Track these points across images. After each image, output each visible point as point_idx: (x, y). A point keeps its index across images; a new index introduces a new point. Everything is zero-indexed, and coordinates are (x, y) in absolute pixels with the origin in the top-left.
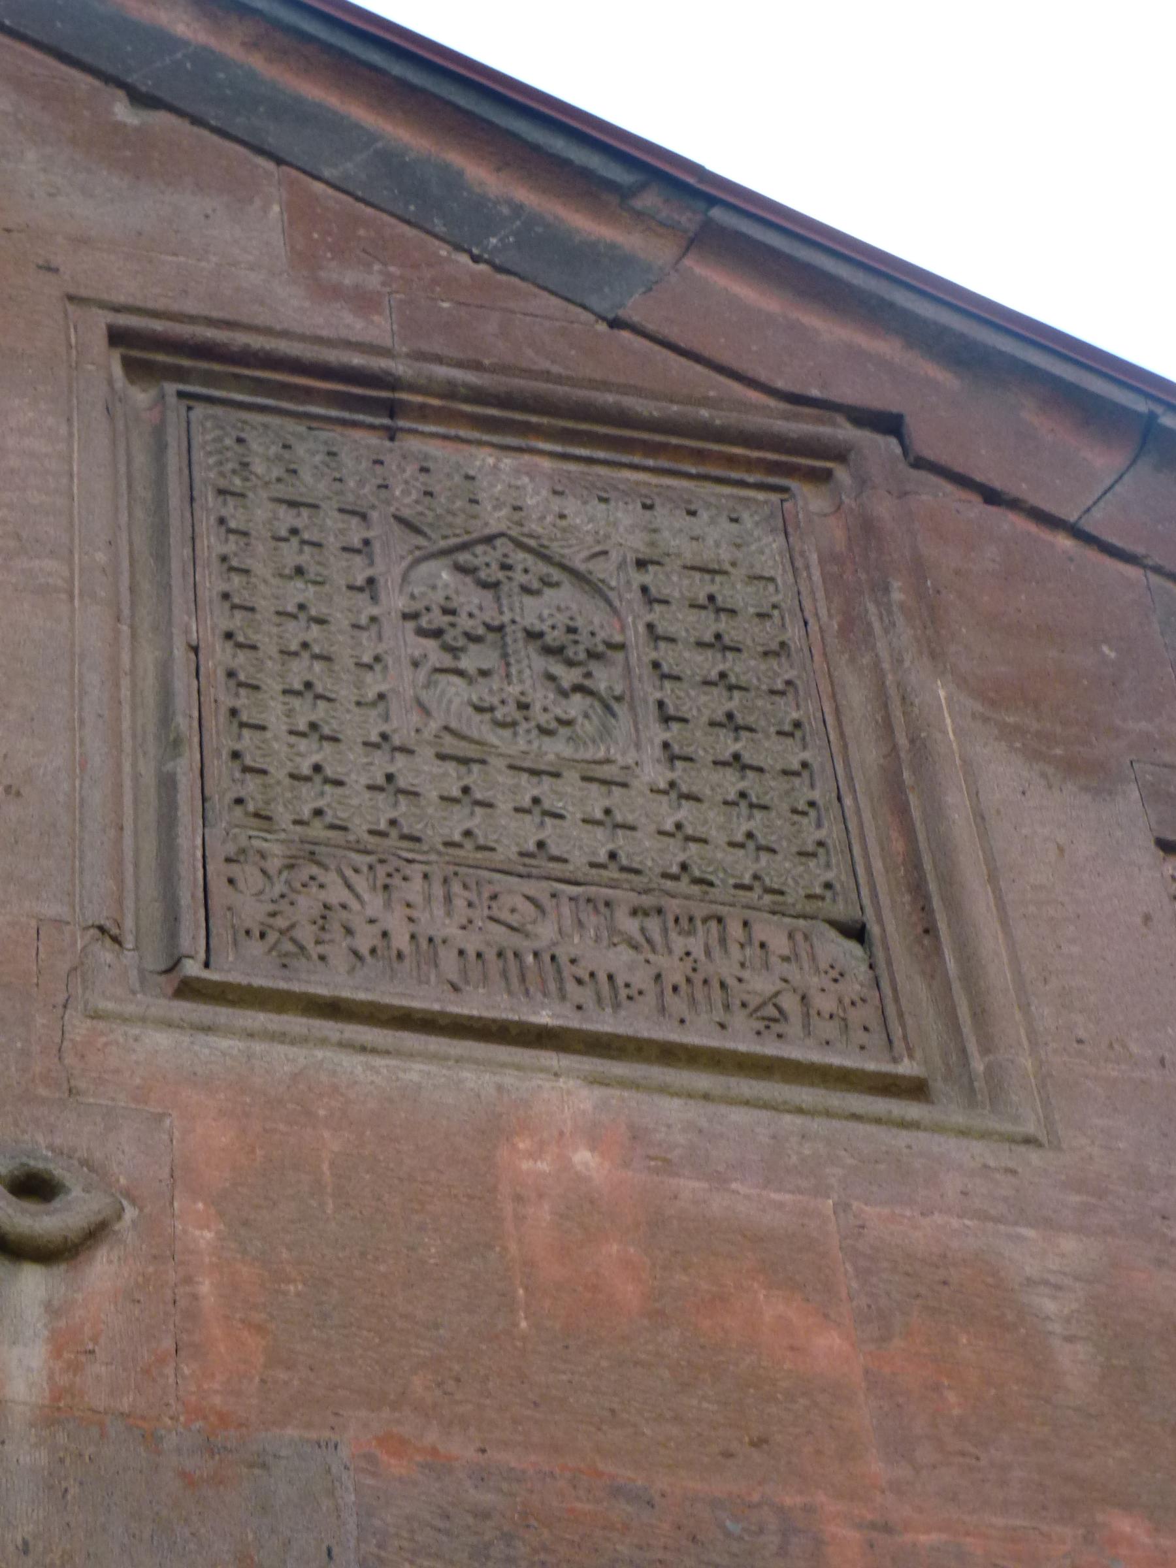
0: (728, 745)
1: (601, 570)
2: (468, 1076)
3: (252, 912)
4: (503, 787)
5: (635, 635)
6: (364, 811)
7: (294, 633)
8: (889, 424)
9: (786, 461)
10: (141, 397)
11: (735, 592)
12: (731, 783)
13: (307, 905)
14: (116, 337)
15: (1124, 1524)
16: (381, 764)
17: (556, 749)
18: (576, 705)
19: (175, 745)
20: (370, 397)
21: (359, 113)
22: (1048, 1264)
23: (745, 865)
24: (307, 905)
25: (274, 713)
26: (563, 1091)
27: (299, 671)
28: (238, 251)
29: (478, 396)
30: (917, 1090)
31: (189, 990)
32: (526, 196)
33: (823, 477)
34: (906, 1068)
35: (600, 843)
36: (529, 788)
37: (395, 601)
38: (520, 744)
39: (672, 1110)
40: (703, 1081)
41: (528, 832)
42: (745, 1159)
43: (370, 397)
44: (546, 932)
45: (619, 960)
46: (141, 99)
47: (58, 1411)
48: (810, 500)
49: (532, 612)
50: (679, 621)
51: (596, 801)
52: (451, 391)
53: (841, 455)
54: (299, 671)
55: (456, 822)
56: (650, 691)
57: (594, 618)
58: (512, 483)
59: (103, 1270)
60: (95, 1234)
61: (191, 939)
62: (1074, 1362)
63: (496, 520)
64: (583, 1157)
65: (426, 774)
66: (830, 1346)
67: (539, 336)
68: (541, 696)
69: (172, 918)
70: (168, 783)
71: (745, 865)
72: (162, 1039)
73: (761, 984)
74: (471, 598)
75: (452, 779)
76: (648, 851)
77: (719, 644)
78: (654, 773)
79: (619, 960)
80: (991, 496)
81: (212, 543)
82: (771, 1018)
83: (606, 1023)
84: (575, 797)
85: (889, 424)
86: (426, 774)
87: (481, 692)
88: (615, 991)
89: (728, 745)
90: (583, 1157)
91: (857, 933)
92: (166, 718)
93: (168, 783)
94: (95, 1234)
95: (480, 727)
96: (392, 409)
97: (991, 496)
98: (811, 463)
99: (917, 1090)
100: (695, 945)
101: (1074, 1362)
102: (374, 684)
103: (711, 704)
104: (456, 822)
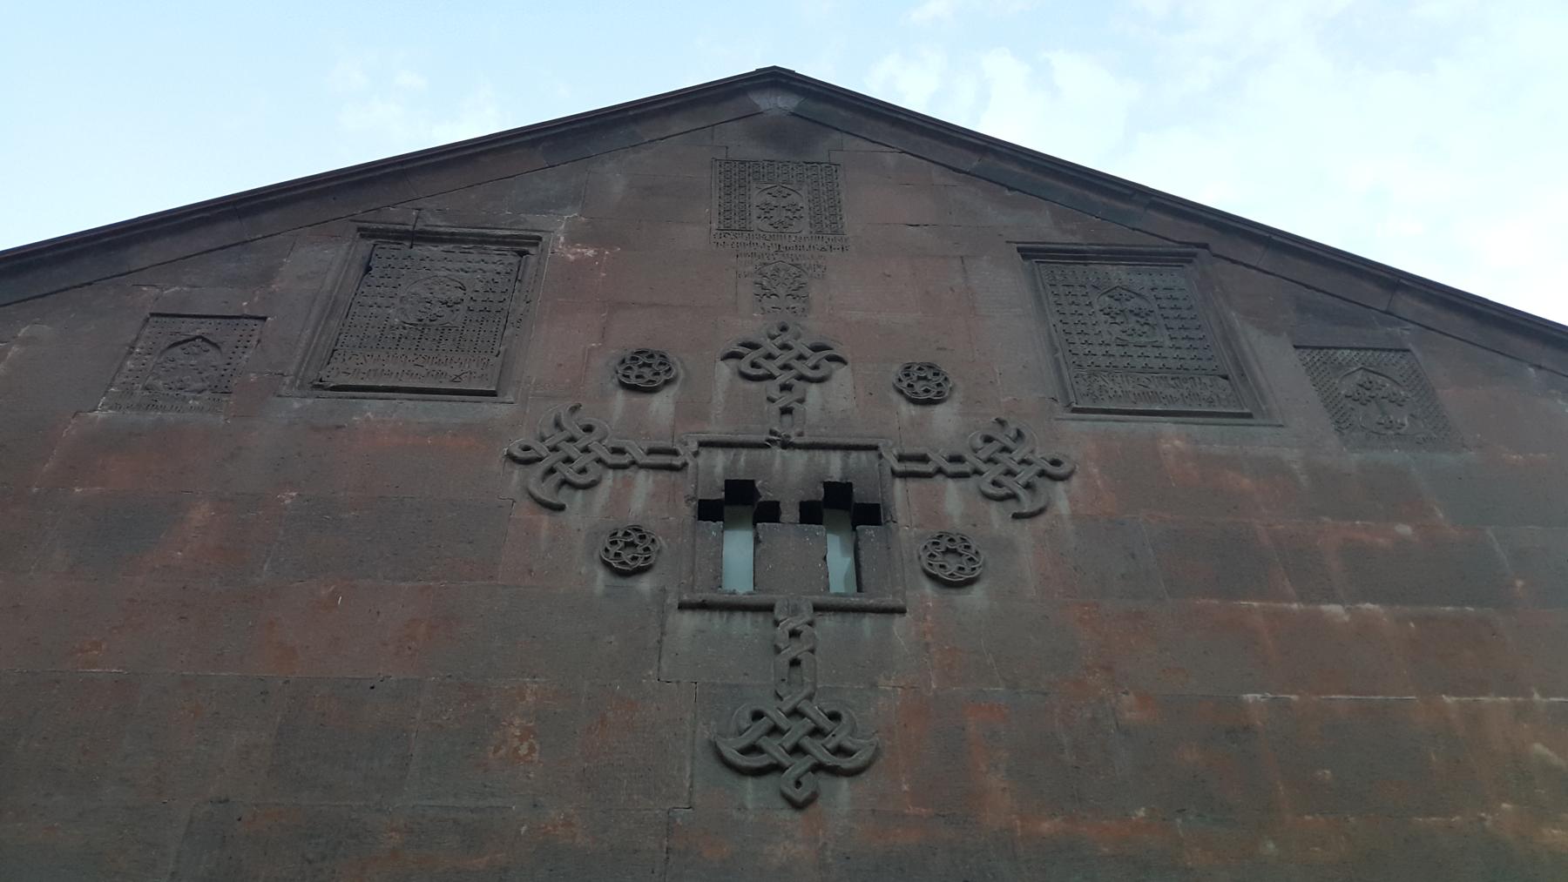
0: (1185, 334)
1: (1144, 292)
2: (1146, 425)
3: (1084, 389)
4: (1131, 350)
5: (1155, 308)
6: (1104, 362)
7: (1076, 319)
8: (1205, 246)
9: (1182, 258)
10: (1027, 263)
11: (1176, 294)
12: (1186, 343)
13: (1096, 386)
14: (1019, 250)
15: (1326, 519)
16: (1104, 349)
17: (1143, 340)
18: (1146, 328)
19: (1056, 350)
20: (1077, 256)
21: (1061, 184)
22: (1291, 456)
23: (1196, 364)
24: (1096, 386)
25: (1076, 339)
26: (1168, 427)
27: (1080, 328)
28: (1042, 225)
29: (1104, 252)
30: (1249, 416)
31: (1075, 410)
32: (1105, 200)
33: (1190, 262)
34: (1246, 410)
35: (1160, 362)
36: (1140, 351)
37: (1097, 307)
38: (1136, 339)
39: (1195, 429)
40: (1201, 420)
41: (1142, 362)
42: (1216, 439)
43: (1077, 256)
44: (1152, 387)
45: (1171, 391)
46: (1010, 189)
47: (1074, 516)
48: (1189, 268)
49: (1129, 305)
50: (1164, 303)
51: (1157, 352)
52: (1098, 252)
53: (1195, 255)
54: (1080, 328)
55: (1125, 361)
56: (1162, 322)
57: (1144, 305)
58: (1118, 274)
59: (1075, 481)
60: (1072, 473)
61: (1072, 398)
62: (1303, 478)
63: (1115, 283)
64: (1177, 443)
65: (1114, 350)
66: (1246, 482)
67: (1116, 235)
68: (1137, 327)
69: (1067, 396)
70: (1057, 360)
71: (1196, 364)
72: (1073, 424)
73: (1207, 394)
74: (1115, 304)
75: (1122, 351)
76: (1171, 363)
77: (1176, 308)
78: (1168, 343)
79: (1171, 391)
80: (1234, 262)
81: (1052, 298)
82: (1211, 402)
83: (1172, 408)
84: (1149, 351)
85: (1205, 246)
86: (1114, 350)
87: (1122, 327)
88: (1172, 400)
89: (1185, 334)
90: (1177, 443)
91: (1226, 378)
92: (1052, 344)
93: (1057, 360)
94: (1072, 473)
95: (1124, 336)
96: (1085, 258)
97: (1234, 262)
98: (1187, 258)
99: (1249, 416)
100: (1188, 385)
101: (1303, 478)
102: (1098, 329)
103: (1175, 324)
104: (1125, 361)
